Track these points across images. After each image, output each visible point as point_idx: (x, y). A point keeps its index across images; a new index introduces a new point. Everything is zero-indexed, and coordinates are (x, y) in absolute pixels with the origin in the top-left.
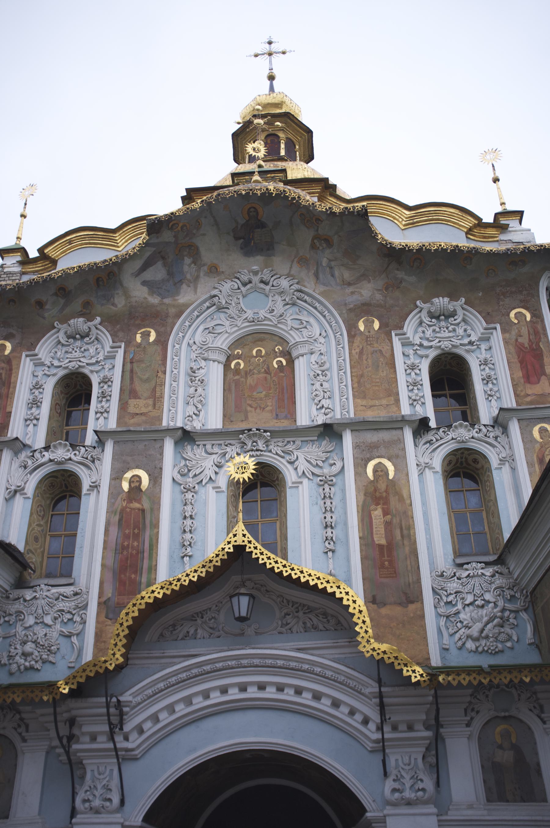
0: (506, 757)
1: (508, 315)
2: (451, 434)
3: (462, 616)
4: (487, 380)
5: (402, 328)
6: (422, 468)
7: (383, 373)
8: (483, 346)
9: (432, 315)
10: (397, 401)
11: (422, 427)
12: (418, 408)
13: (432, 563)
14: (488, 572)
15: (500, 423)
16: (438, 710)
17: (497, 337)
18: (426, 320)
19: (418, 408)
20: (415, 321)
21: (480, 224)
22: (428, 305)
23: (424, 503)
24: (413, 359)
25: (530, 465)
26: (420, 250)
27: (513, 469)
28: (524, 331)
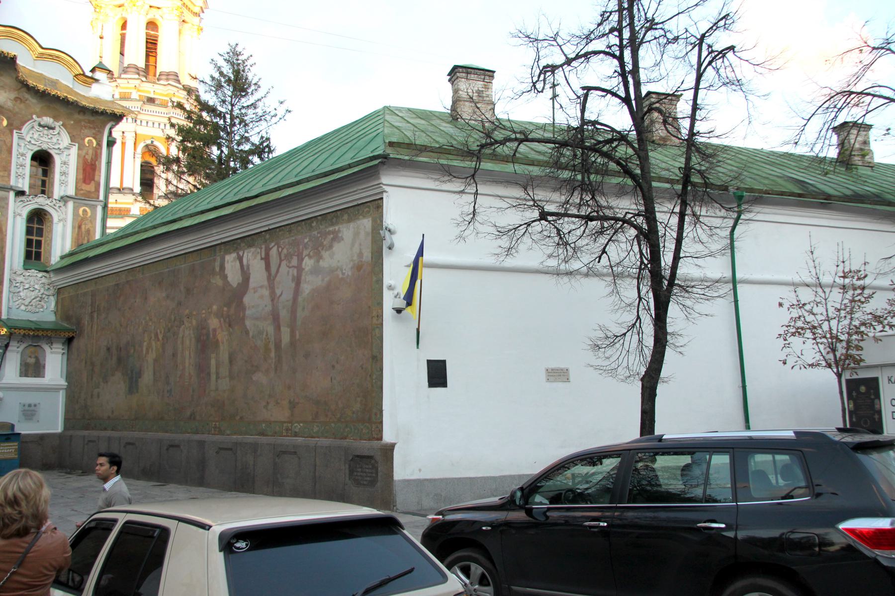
0: (32, 361)
1: (84, 139)
2: (36, 200)
3: (21, 294)
4: (63, 174)
5: (20, 129)
6: (15, 215)
7: (4, 155)
8: (65, 153)
9: (40, 125)
10: (9, 175)
11: (20, 193)
12: (20, 180)
13: (11, 266)
14: (40, 274)
15: (64, 199)
16: (8, 344)
17: (74, 150)
18: (37, 127)
19: (20, 180)
20: (30, 127)
21: (84, 75)
22: (40, 119)
23: (13, 234)
24: (22, 150)
25: (73, 227)
26: (44, 92)
27: (64, 226)
28: (90, 152)
